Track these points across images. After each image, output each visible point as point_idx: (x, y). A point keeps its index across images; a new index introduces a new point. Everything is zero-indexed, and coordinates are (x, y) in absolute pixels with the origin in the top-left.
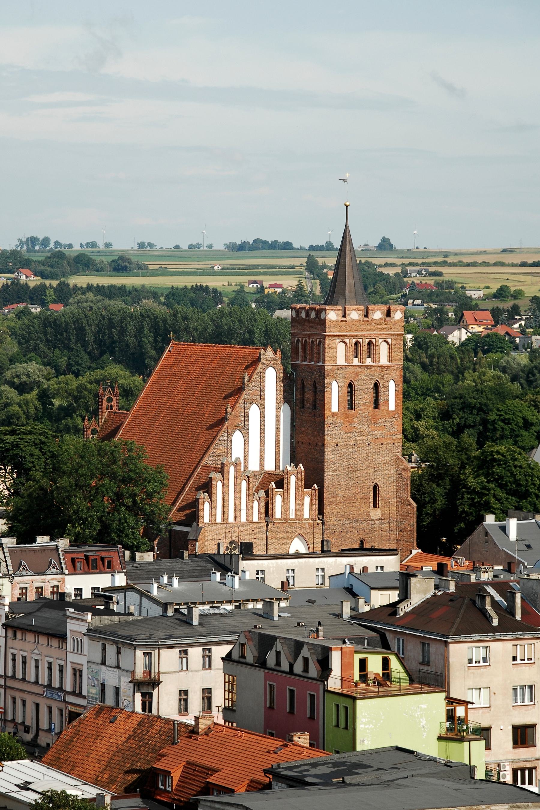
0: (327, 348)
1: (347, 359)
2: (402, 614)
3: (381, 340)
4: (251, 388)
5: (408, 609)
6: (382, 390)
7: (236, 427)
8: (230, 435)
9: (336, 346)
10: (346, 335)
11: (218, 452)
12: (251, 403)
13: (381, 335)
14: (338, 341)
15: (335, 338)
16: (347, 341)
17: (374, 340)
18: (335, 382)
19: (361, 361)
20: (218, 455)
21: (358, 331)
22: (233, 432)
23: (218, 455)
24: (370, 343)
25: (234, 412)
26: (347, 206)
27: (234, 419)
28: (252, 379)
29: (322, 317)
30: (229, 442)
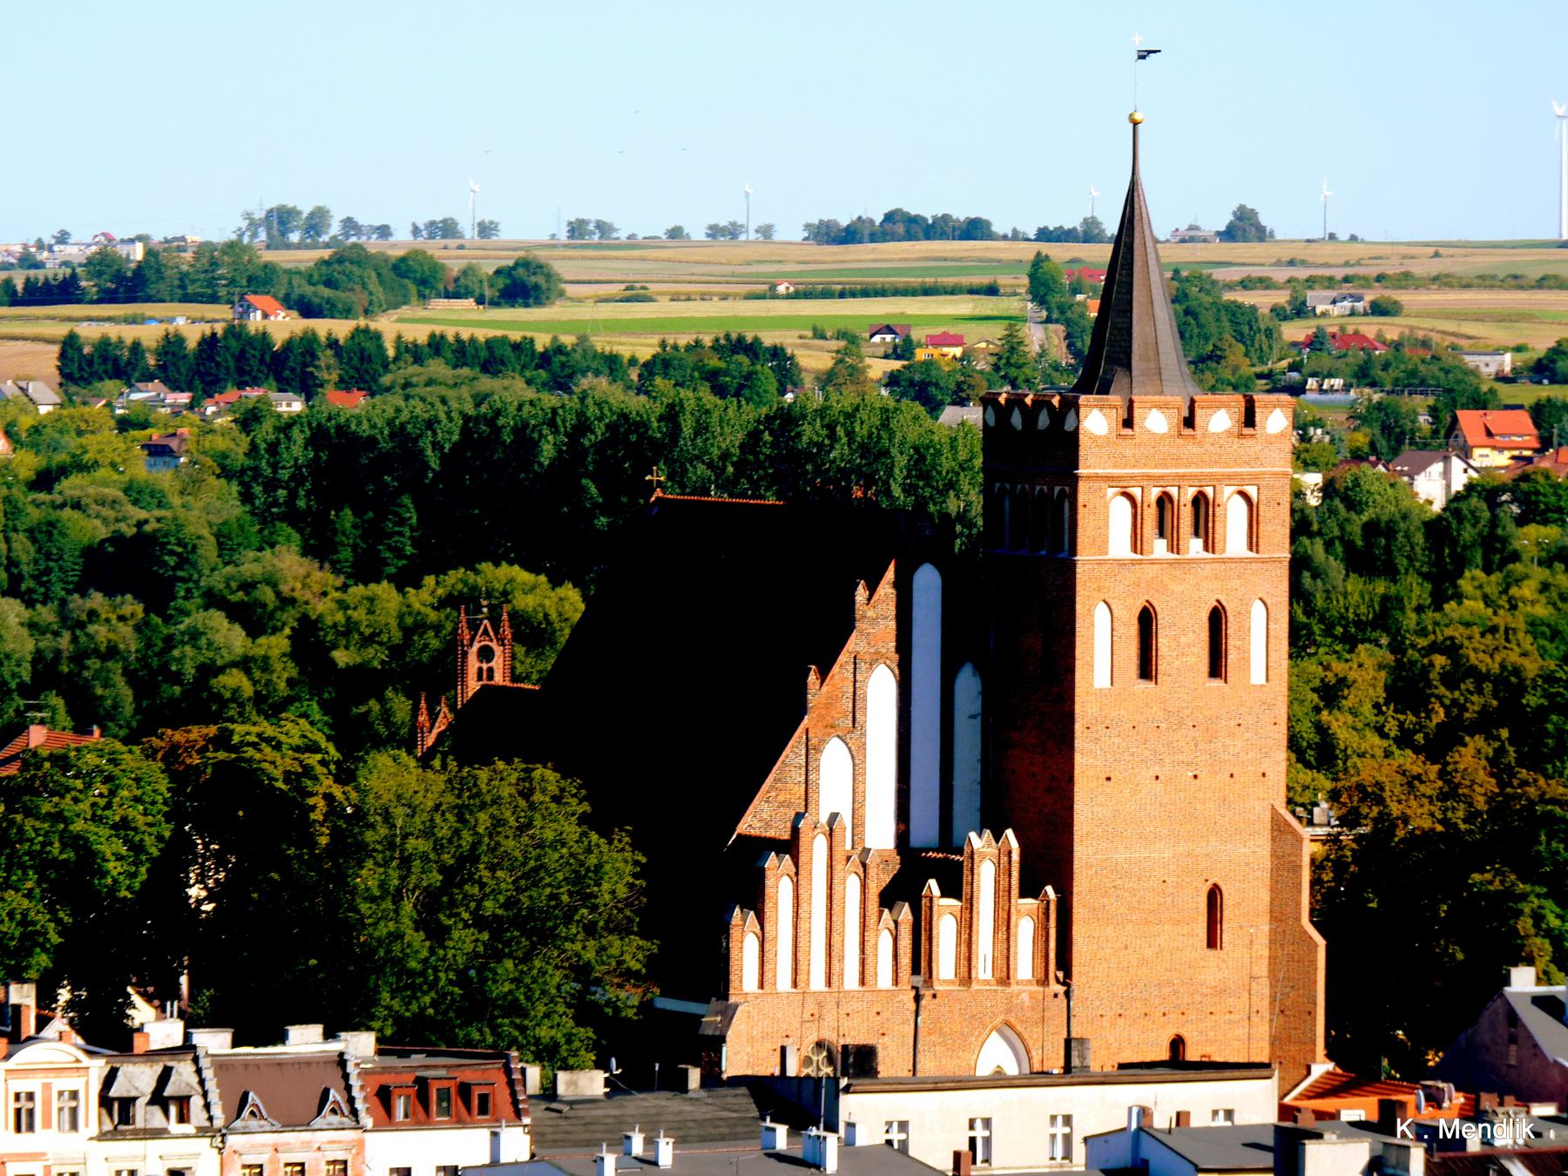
0: (1081, 510)
1: (1137, 543)
3: (1229, 490)
8: (811, 751)
9: (1106, 506)
10: (1133, 477)
11: (781, 798)
13: (1230, 477)
14: (1111, 491)
15: (1103, 485)
16: (1136, 492)
17: (1209, 491)
18: (1102, 606)
19: (1174, 547)
20: (781, 804)
22: (823, 742)
23: (781, 804)
24: (1200, 501)
25: (825, 688)
26: (1135, 124)
27: (828, 706)
28: (876, 597)
29: (1069, 426)
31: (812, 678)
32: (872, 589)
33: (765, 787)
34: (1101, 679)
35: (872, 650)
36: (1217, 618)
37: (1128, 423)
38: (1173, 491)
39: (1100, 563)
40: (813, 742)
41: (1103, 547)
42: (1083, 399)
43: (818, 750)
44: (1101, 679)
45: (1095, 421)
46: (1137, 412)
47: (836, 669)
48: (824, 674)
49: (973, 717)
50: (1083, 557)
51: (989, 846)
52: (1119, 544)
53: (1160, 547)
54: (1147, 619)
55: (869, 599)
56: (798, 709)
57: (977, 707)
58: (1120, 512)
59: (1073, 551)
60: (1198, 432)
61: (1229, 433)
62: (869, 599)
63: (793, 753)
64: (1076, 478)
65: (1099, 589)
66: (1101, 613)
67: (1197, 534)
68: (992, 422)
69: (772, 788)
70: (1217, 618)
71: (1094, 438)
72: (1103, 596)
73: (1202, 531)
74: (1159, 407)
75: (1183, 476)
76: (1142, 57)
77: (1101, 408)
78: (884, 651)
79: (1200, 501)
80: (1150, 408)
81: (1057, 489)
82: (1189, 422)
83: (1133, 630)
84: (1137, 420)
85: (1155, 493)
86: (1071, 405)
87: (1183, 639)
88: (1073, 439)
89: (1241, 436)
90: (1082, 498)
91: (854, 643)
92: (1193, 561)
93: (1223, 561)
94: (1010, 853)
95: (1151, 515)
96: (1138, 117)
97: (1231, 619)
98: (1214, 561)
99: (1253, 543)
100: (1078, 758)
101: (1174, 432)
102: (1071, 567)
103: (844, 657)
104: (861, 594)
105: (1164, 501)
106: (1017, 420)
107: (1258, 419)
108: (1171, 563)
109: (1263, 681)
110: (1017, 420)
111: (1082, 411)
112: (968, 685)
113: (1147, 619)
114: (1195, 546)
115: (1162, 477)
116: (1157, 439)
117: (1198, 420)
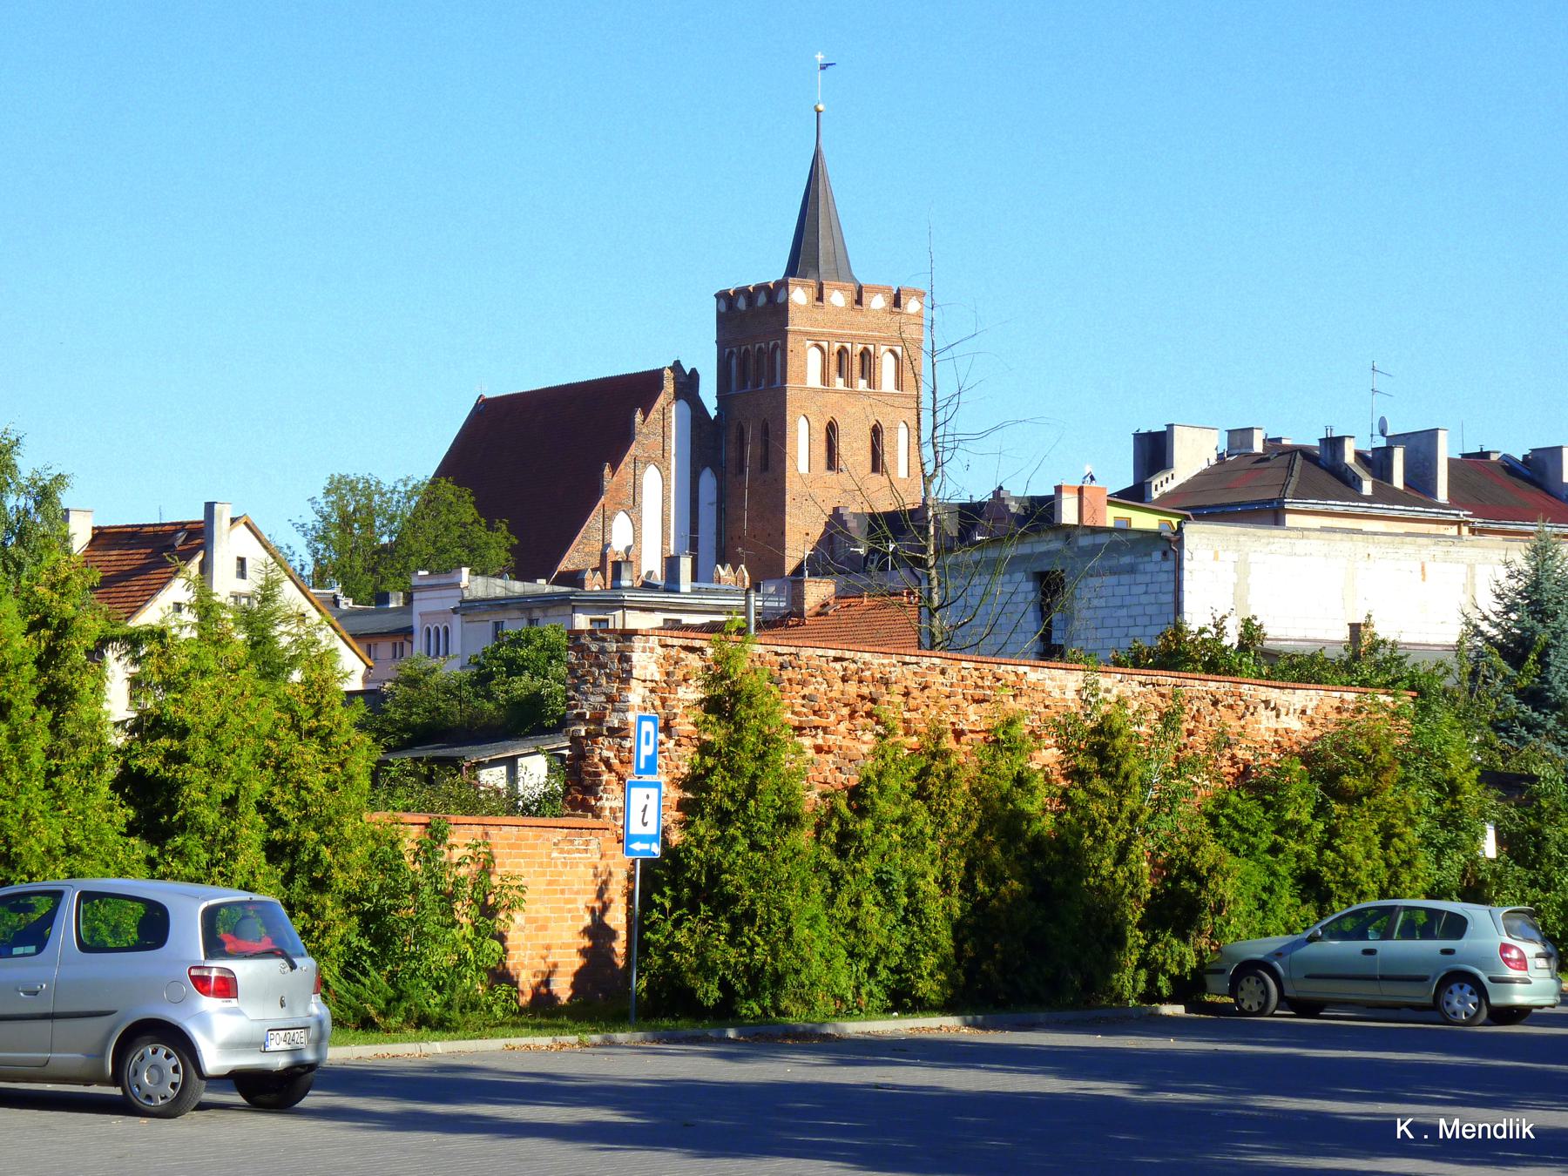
0: (789, 353)
1: (825, 379)
2: (1155, 495)
3: (884, 348)
4: (647, 436)
5: (1168, 487)
6: (886, 438)
7: (619, 506)
8: (607, 519)
9: (805, 352)
10: (823, 334)
11: (586, 550)
12: (646, 464)
13: (884, 339)
14: (809, 343)
15: (805, 338)
16: (825, 345)
17: (871, 348)
18: (803, 418)
19: (849, 383)
20: (586, 554)
21: (843, 328)
22: (614, 514)
23: (586, 554)
24: (865, 354)
25: (615, 478)
26: (818, 112)
27: (617, 490)
28: (648, 420)
29: (780, 300)
30: (605, 530)
31: (607, 471)
32: (646, 414)
33: (576, 542)
34: (803, 467)
35: (646, 455)
36: (876, 431)
37: (820, 298)
38: (848, 346)
39: (802, 390)
40: (608, 513)
41: (804, 380)
42: (791, 280)
43: (611, 519)
44: (803, 467)
45: (799, 296)
46: (825, 291)
47: (622, 466)
48: (614, 468)
49: (712, 504)
50: (791, 384)
51: (730, 575)
52: (814, 380)
53: (839, 383)
54: (831, 429)
55: (644, 421)
56: (595, 491)
57: (714, 498)
58: (814, 358)
59: (784, 380)
60: (865, 307)
61: (884, 310)
62: (644, 421)
63: (594, 520)
64: (786, 333)
65: (801, 407)
66: (802, 422)
67: (863, 377)
68: (723, 309)
69: (580, 542)
70: (876, 431)
71: (798, 306)
72: (803, 412)
73: (867, 374)
74: (840, 289)
75: (854, 336)
76: (824, 68)
77: (803, 287)
78: (653, 456)
79: (865, 354)
80: (833, 289)
81: (771, 344)
82: (859, 301)
83: (823, 436)
84: (825, 297)
85: (837, 346)
86: (782, 285)
87: (855, 445)
88: (784, 308)
89: (891, 312)
90: (790, 346)
91: (633, 450)
92: (860, 393)
93: (880, 394)
94: (744, 579)
95: (834, 360)
96: (821, 107)
97: (885, 433)
98: (875, 394)
99: (899, 384)
100: (787, 518)
101: (849, 306)
102: (783, 391)
103: (627, 458)
104: (638, 417)
105: (842, 352)
106: (742, 304)
107: (902, 302)
108: (847, 393)
109: (906, 476)
110: (742, 304)
111: (790, 287)
112: (708, 481)
113: (831, 429)
114: (862, 385)
115: (841, 335)
116: (838, 310)
117: (864, 300)
